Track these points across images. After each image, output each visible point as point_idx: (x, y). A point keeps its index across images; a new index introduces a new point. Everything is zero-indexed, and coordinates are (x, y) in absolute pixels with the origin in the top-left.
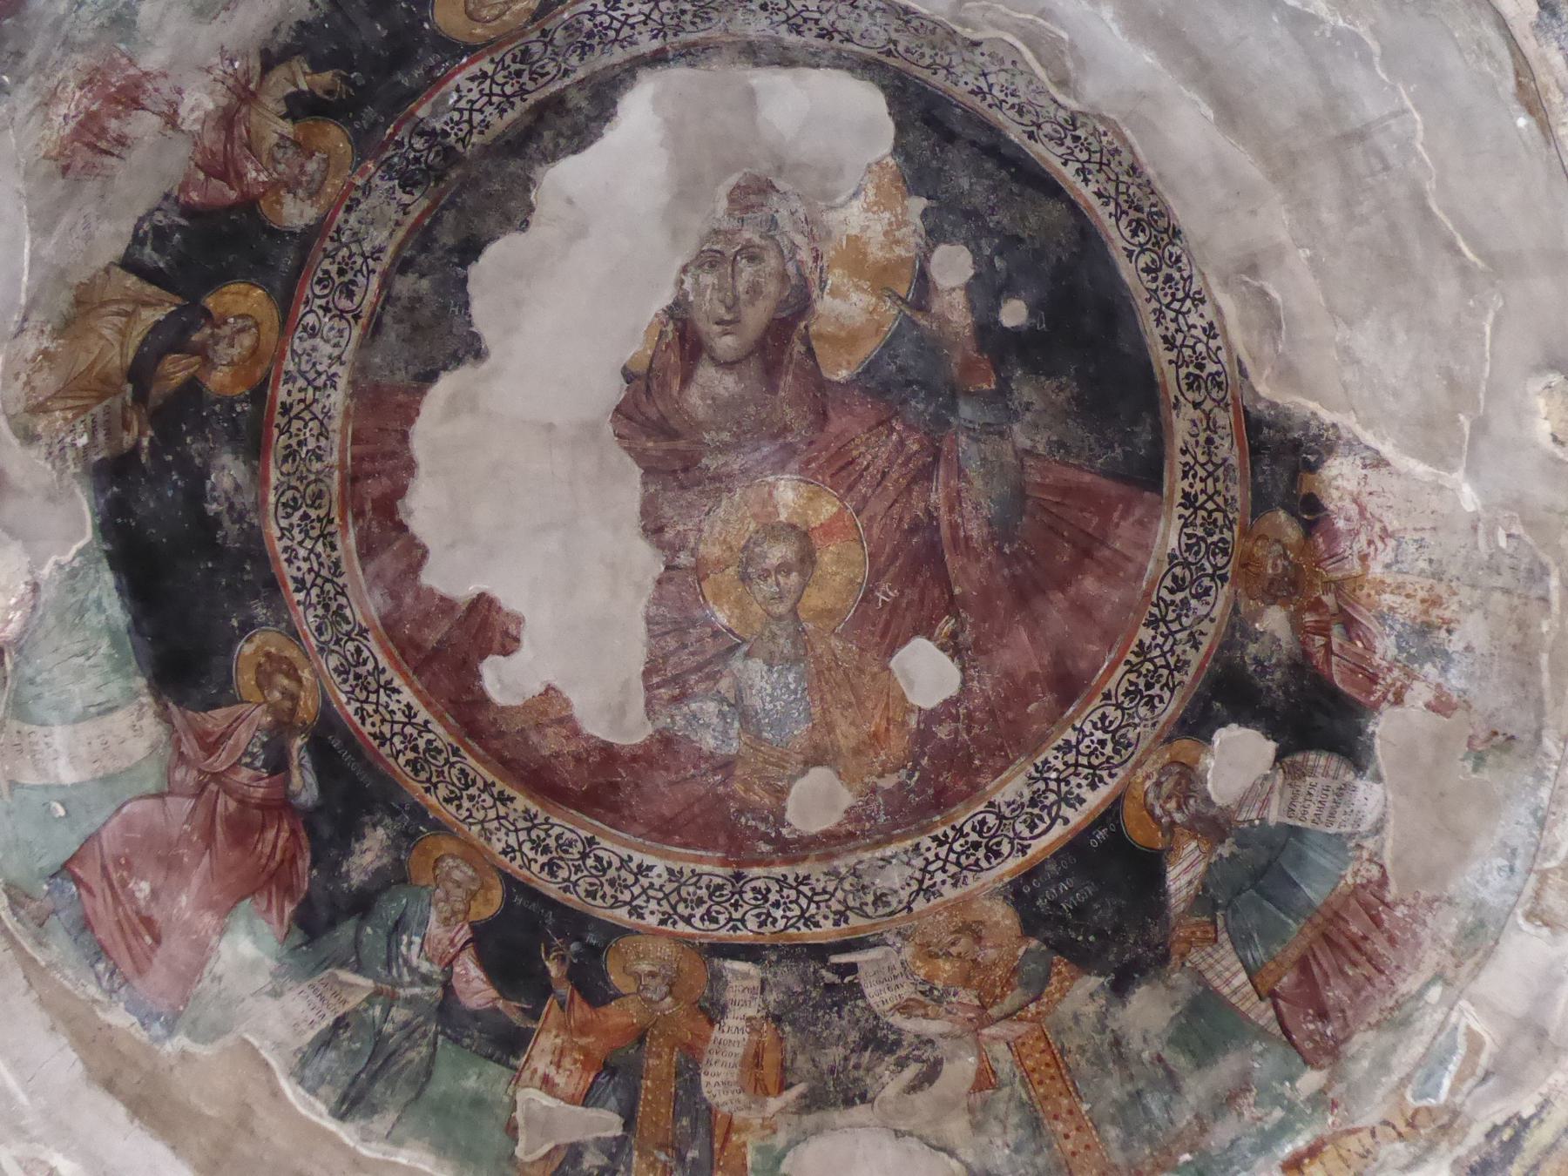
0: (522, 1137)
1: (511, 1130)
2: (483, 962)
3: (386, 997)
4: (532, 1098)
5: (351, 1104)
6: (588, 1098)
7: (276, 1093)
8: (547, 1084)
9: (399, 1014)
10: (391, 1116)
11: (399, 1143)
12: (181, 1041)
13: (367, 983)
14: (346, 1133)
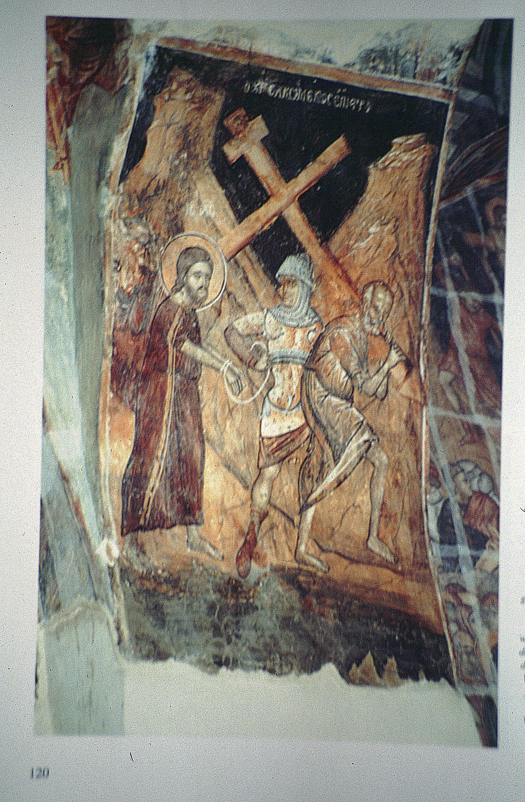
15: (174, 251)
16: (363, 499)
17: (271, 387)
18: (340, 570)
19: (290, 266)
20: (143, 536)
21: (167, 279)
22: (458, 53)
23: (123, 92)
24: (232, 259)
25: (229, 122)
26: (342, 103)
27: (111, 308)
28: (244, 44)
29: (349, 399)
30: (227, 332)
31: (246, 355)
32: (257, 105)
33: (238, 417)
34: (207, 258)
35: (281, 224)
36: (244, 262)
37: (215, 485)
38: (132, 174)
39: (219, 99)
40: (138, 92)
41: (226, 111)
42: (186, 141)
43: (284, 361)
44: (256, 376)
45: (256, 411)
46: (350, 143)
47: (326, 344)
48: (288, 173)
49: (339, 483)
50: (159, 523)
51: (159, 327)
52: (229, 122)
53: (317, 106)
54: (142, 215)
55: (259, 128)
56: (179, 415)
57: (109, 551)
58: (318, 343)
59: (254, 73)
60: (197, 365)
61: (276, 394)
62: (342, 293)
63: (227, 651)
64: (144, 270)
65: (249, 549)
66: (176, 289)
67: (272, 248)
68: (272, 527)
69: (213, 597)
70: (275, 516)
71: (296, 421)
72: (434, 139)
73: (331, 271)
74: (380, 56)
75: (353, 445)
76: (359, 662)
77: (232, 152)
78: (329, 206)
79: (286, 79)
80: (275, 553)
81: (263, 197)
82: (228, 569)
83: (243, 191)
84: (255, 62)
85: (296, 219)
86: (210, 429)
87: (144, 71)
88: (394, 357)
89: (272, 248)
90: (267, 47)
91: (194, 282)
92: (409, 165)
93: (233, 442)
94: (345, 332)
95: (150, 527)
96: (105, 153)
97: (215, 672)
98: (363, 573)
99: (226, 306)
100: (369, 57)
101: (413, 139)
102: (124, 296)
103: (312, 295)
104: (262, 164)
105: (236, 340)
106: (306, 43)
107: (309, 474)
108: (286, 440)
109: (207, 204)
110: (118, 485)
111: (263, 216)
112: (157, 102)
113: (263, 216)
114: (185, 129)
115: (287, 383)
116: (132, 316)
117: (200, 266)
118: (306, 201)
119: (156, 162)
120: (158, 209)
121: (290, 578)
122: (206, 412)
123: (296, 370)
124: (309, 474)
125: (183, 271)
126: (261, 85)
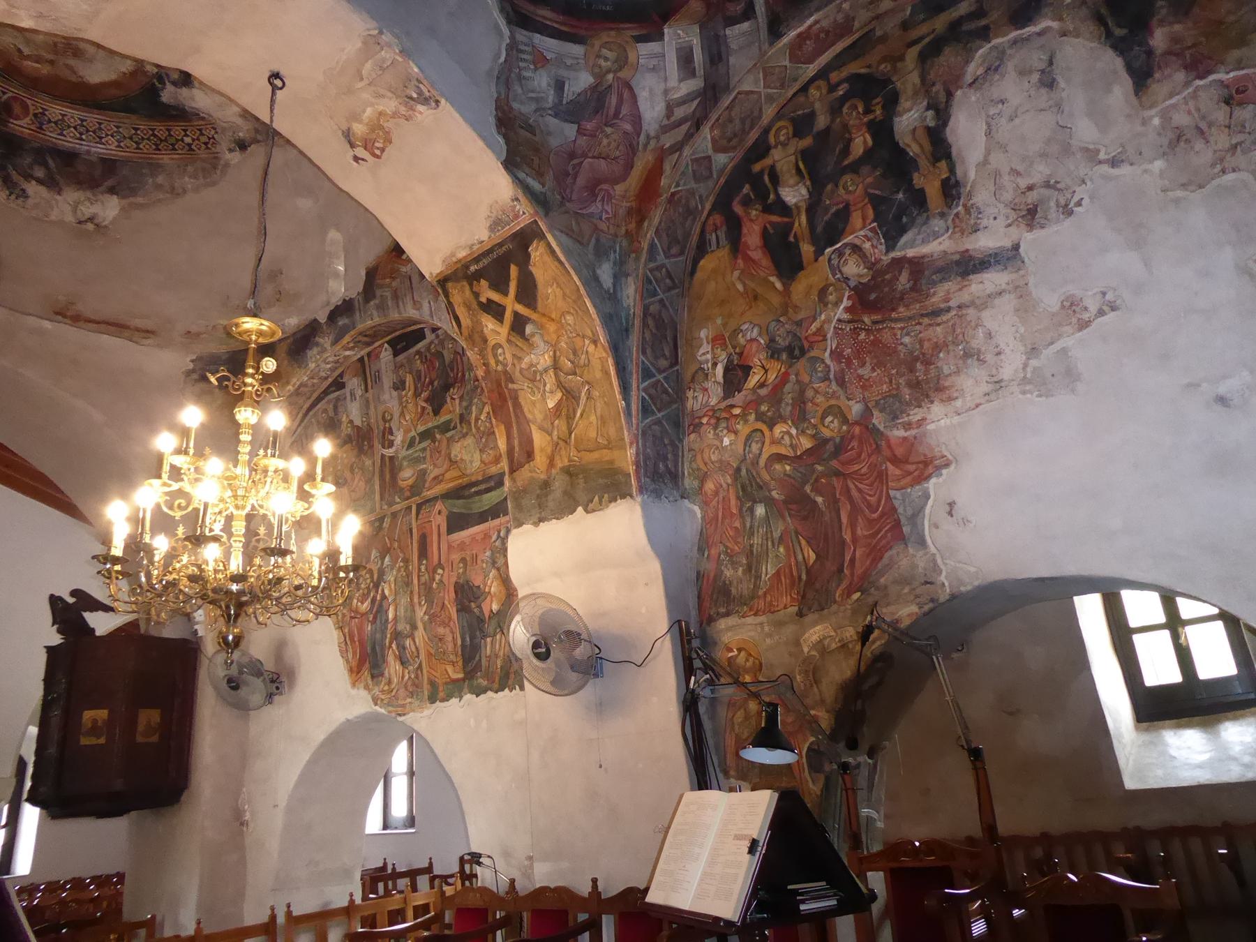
15: (489, 350)
16: (593, 418)
19: (529, 329)
21: (492, 362)
22: (517, 199)
24: (509, 341)
25: (475, 289)
28: (454, 259)
29: (575, 374)
30: (521, 372)
31: (531, 376)
32: (477, 276)
34: (501, 346)
35: (516, 315)
37: (539, 439)
41: (471, 285)
42: (468, 307)
43: (546, 370)
45: (544, 399)
46: (516, 265)
48: (506, 293)
49: (582, 415)
50: (521, 466)
51: (499, 385)
52: (475, 289)
53: (494, 260)
56: (516, 416)
59: (466, 267)
65: (551, 464)
67: (518, 325)
71: (559, 395)
72: (542, 237)
73: (544, 320)
74: (495, 225)
77: (483, 300)
78: (528, 292)
79: (477, 260)
80: (561, 462)
81: (504, 308)
85: (520, 309)
86: (529, 416)
88: (587, 342)
89: (518, 325)
90: (462, 254)
91: (501, 358)
92: (541, 255)
93: (539, 417)
94: (563, 344)
98: (596, 455)
100: (493, 228)
103: (542, 336)
104: (495, 296)
105: (525, 373)
106: (470, 243)
108: (558, 405)
109: (489, 324)
111: (508, 316)
113: (508, 316)
115: (550, 379)
117: (500, 351)
118: (519, 299)
119: (465, 321)
120: (476, 336)
122: (526, 410)
123: (551, 372)
124: (570, 418)
125: (495, 356)
126: (473, 268)
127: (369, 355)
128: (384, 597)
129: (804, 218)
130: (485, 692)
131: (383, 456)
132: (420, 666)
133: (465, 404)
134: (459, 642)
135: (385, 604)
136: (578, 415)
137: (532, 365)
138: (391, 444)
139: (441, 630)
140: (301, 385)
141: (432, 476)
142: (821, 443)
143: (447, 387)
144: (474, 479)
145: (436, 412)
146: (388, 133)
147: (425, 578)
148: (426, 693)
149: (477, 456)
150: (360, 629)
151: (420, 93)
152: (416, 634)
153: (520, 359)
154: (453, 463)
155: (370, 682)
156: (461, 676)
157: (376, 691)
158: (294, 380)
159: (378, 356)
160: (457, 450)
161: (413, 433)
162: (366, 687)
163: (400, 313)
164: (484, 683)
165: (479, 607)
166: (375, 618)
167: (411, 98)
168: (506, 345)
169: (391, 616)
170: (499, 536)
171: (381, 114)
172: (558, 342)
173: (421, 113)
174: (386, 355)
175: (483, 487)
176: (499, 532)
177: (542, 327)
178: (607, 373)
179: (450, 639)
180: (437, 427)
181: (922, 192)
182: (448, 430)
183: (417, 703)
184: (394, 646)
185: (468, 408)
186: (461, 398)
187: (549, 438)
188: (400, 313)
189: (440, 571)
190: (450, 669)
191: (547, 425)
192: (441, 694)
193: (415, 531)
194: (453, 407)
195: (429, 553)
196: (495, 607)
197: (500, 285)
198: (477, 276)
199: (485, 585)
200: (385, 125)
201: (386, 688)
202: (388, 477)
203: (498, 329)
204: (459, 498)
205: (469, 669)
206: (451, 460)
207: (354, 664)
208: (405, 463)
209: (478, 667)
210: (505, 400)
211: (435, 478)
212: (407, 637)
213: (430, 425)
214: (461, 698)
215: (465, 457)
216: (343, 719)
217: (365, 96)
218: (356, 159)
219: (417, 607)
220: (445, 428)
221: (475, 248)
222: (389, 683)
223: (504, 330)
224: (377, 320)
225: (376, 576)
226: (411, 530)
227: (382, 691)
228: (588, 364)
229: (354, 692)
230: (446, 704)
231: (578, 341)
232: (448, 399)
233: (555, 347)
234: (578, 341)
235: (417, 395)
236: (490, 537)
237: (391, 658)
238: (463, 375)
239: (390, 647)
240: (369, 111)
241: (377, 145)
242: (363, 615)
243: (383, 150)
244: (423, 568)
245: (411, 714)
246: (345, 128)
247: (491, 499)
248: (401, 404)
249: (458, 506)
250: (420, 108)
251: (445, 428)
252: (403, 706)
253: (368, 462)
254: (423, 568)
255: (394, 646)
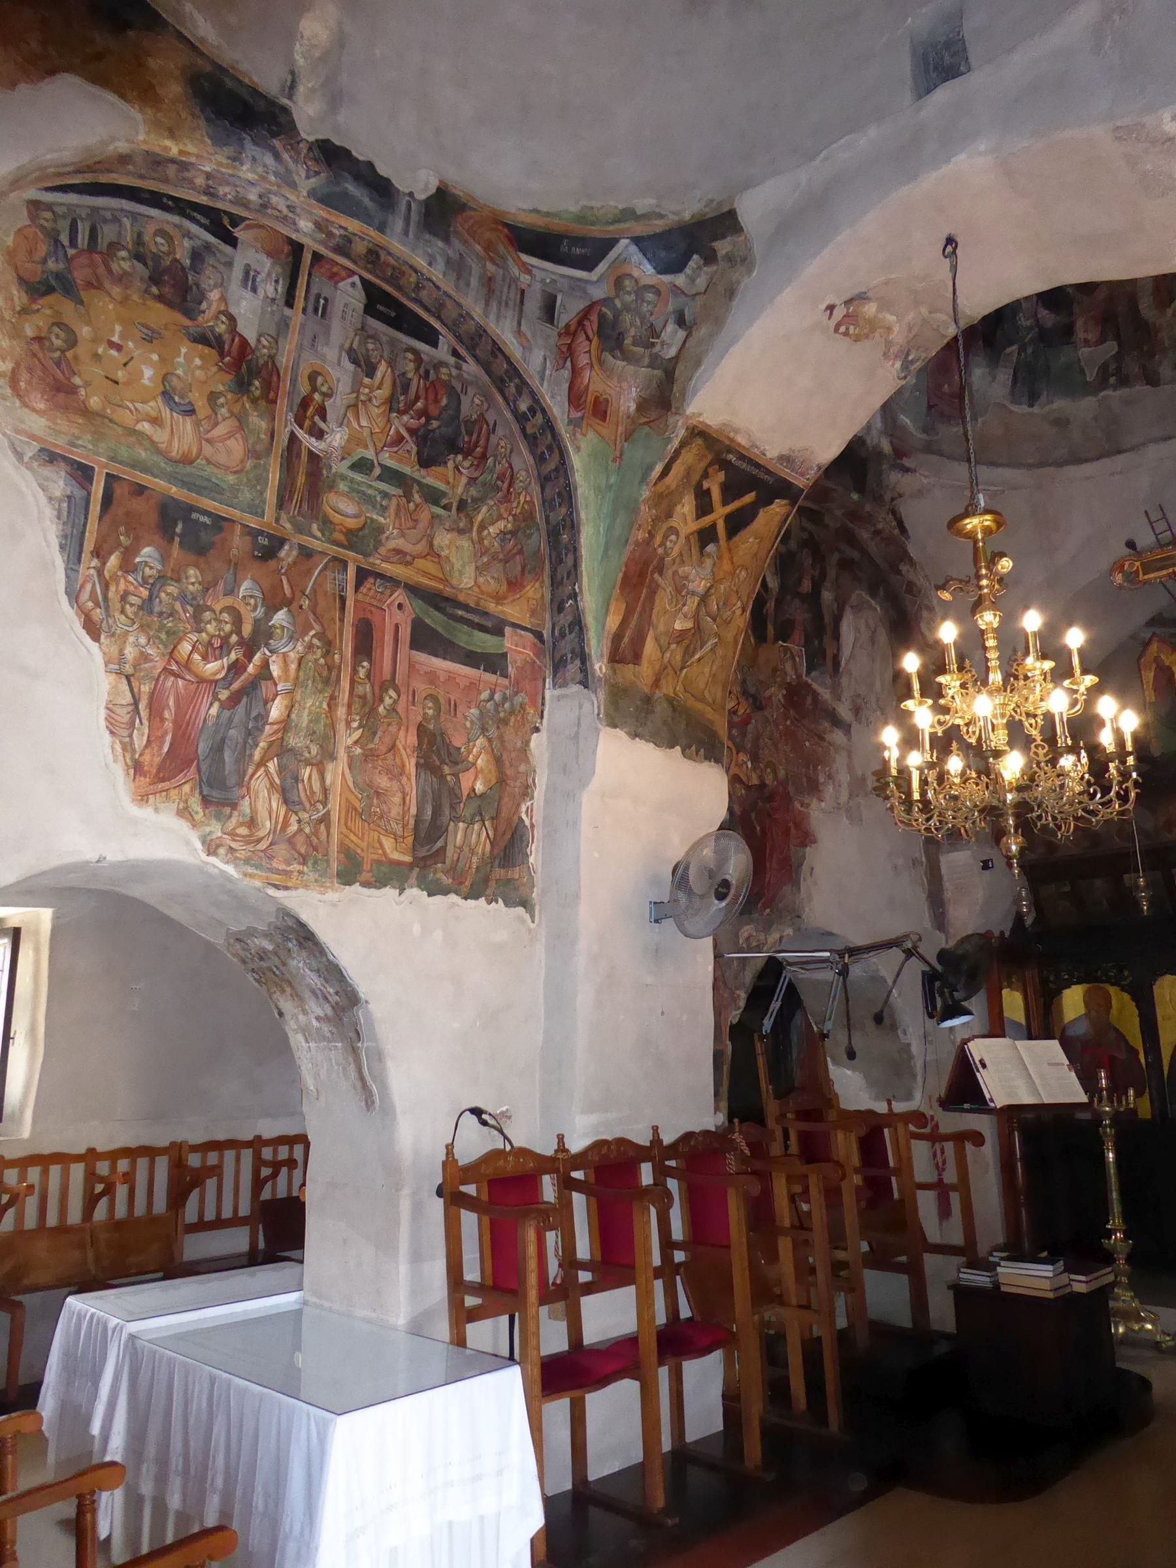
0: (1087, 372)
1: (1082, 372)
2: (1046, 307)
3: (1023, 348)
4: (1084, 352)
5: (1033, 399)
6: (1102, 340)
7: (1011, 412)
8: (1087, 343)
9: (1030, 351)
10: (1045, 393)
11: (1052, 402)
12: (980, 420)
13: (1015, 347)
14: (1036, 409)
15: (665, 527)
16: (707, 670)
17: (684, 605)
18: (691, 702)
19: (711, 548)
20: (617, 666)
21: (658, 540)
22: (820, 468)
23: (669, 440)
24: (687, 538)
25: (710, 470)
26: (762, 475)
27: (630, 548)
28: (732, 434)
29: (714, 620)
32: (725, 465)
33: (667, 616)
34: (677, 534)
35: (714, 526)
36: (692, 541)
37: (650, 647)
38: (660, 484)
39: (710, 457)
40: (676, 443)
41: (710, 465)
42: (688, 474)
43: (693, 593)
44: (680, 598)
45: (674, 616)
46: (757, 496)
47: (713, 591)
49: (699, 660)
51: (646, 564)
54: (657, 505)
55: (721, 476)
56: (643, 608)
57: (601, 668)
58: (710, 588)
59: (729, 450)
60: (658, 586)
61: (686, 608)
62: (727, 566)
63: (640, 730)
64: (650, 532)
65: (656, 683)
66: (660, 546)
68: (668, 674)
69: (639, 703)
70: (670, 669)
71: (689, 625)
73: (726, 555)
74: (786, 459)
75: (710, 643)
76: (690, 747)
77: (706, 485)
78: (737, 523)
79: (742, 457)
80: (667, 688)
81: (711, 511)
82: (646, 690)
83: (704, 506)
84: (733, 445)
87: (682, 432)
89: (706, 536)
90: (741, 440)
93: (662, 628)
95: (619, 662)
96: (651, 468)
97: (634, 739)
98: (699, 706)
99: (677, 561)
100: (782, 458)
101: (784, 502)
102: (637, 544)
103: (714, 565)
105: (677, 578)
107: (688, 653)
108: (683, 633)
109: (687, 506)
110: (611, 637)
111: (707, 520)
112: (683, 451)
113: (707, 520)
114: (690, 468)
115: (692, 603)
116: (637, 554)
117: (673, 537)
118: (728, 518)
119: (672, 479)
120: (663, 506)
121: (670, 701)
122: (655, 611)
123: (697, 599)
124: (688, 653)
125: (666, 537)
126: (731, 457)
127: (317, 257)
128: (264, 671)
129: (773, 604)
130: (445, 892)
131: (293, 437)
132: (325, 819)
133: (473, 492)
134: (413, 810)
135: (265, 688)
136: (697, 656)
137: (686, 578)
138: (320, 435)
139: (383, 782)
140: (184, 166)
141: (392, 544)
142: (762, 786)
143: (453, 446)
144: (462, 598)
145: (425, 462)
146: (867, 336)
147: (365, 689)
148: (335, 866)
149: (470, 570)
150: (185, 705)
151: (912, 362)
152: (330, 767)
153: (683, 562)
154: (432, 553)
155: (195, 804)
156: (407, 859)
157: (215, 829)
158: (191, 148)
159: (334, 278)
160: (443, 539)
161: (370, 454)
162: (184, 813)
163: (486, 313)
164: (446, 880)
165: (456, 775)
166: (234, 700)
167: (908, 355)
168: (682, 540)
169: (276, 711)
170: (491, 698)
171: (889, 329)
172: (720, 581)
173: (893, 365)
174: (348, 296)
175: (477, 619)
176: (493, 693)
177: (720, 558)
178: (736, 643)
179: (397, 799)
180: (419, 483)
181: (825, 650)
182: (436, 503)
183: (312, 876)
184: (272, 766)
185: (479, 501)
186: (472, 481)
187: (659, 654)
188: (486, 313)
189: (392, 693)
190: (388, 843)
191: (664, 641)
192: (365, 876)
193: (350, 603)
194: (454, 478)
195: (376, 654)
196: (479, 787)
197: (730, 492)
198: (725, 465)
199: (469, 752)
200: (877, 335)
201: (243, 831)
202: (301, 479)
203: (689, 519)
204: (437, 608)
205: (423, 852)
206: (431, 545)
207: (152, 760)
208: (342, 487)
209: (441, 853)
210: (642, 584)
211: (398, 551)
212: (308, 763)
213: (407, 470)
214: (402, 891)
215: (453, 560)
216: (90, 855)
217: (911, 316)
218: (831, 308)
219: (341, 727)
220: (433, 497)
221: (756, 450)
222: (252, 823)
223: (693, 526)
224: (437, 273)
225: (247, 629)
226: (343, 600)
227: (233, 834)
228: (728, 623)
229: (146, 813)
230: (365, 891)
231: (734, 599)
232: (450, 464)
233: (715, 582)
234: (734, 599)
235: (391, 403)
236: (480, 693)
237: (259, 784)
238: (484, 457)
239: (262, 763)
240: (891, 318)
241: (852, 328)
242: (201, 680)
243: (846, 334)
244: (362, 673)
245: (301, 891)
246: (870, 294)
247: (483, 642)
248: (356, 390)
249: (435, 619)
250: (898, 365)
251: (433, 497)
252: (287, 873)
253: (258, 422)
254: (362, 673)
255: (272, 766)
